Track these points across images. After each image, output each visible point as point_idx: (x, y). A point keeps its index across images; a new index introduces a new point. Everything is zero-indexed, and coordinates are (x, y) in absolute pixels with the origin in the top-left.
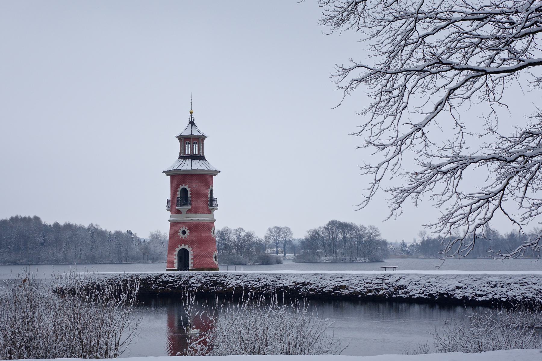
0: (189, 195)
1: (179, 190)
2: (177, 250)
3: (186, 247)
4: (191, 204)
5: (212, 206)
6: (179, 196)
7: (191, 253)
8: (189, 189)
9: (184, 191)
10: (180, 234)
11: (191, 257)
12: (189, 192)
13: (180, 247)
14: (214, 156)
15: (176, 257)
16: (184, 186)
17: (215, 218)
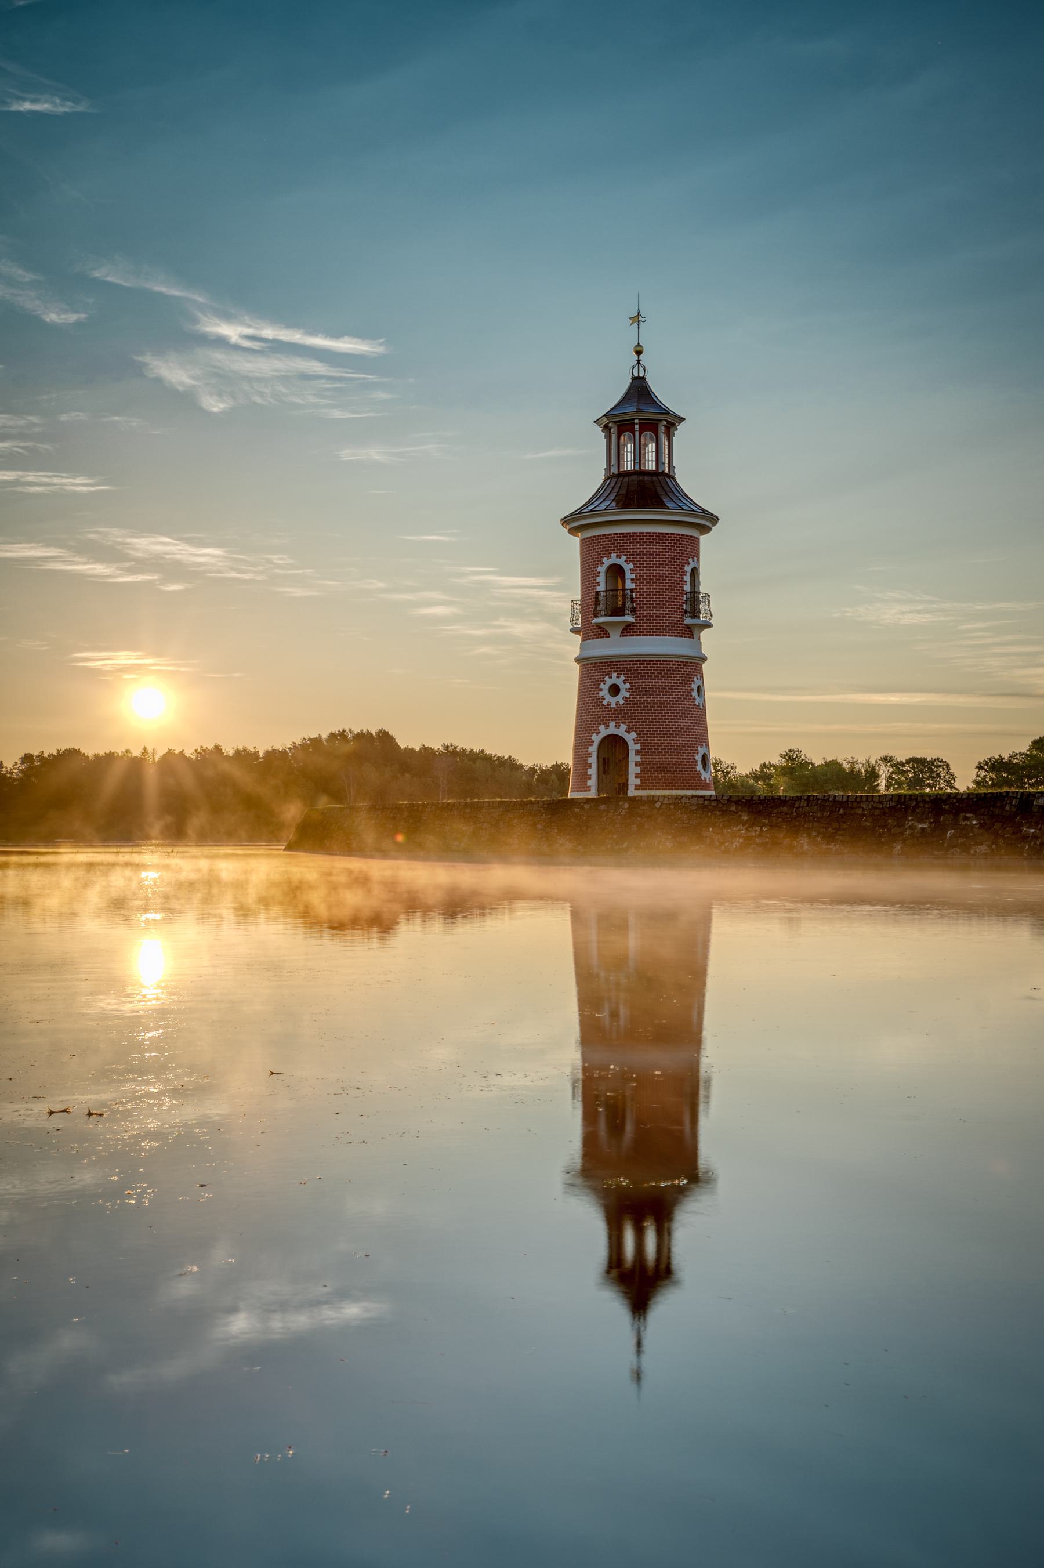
0: (630, 585)
1: (601, 569)
3: (621, 731)
4: (634, 611)
5: (695, 613)
6: (601, 588)
7: (633, 747)
8: (628, 567)
9: (616, 571)
10: (605, 693)
11: (633, 758)
12: (629, 576)
13: (604, 731)
14: (696, 467)
16: (614, 559)
17: (704, 651)
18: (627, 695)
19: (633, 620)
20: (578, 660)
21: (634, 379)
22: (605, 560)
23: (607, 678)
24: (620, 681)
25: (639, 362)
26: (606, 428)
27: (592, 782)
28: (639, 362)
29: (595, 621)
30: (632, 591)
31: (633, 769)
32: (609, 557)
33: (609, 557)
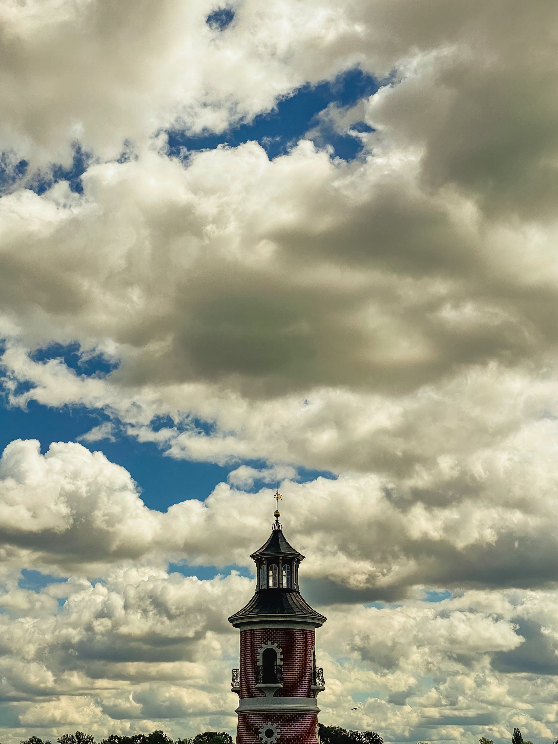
0: (279, 663)
1: (261, 651)
4: (282, 679)
6: (260, 663)
8: (279, 651)
12: (279, 656)
16: (269, 645)
18: (279, 737)
19: (282, 686)
20: (237, 712)
21: (273, 531)
22: (263, 645)
23: (264, 725)
24: (273, 727)
25: (277, 521)
28: (277, 521)
29: (257, 686)
30: (281, 666)
32: (266, 644)
33: (266, 644)
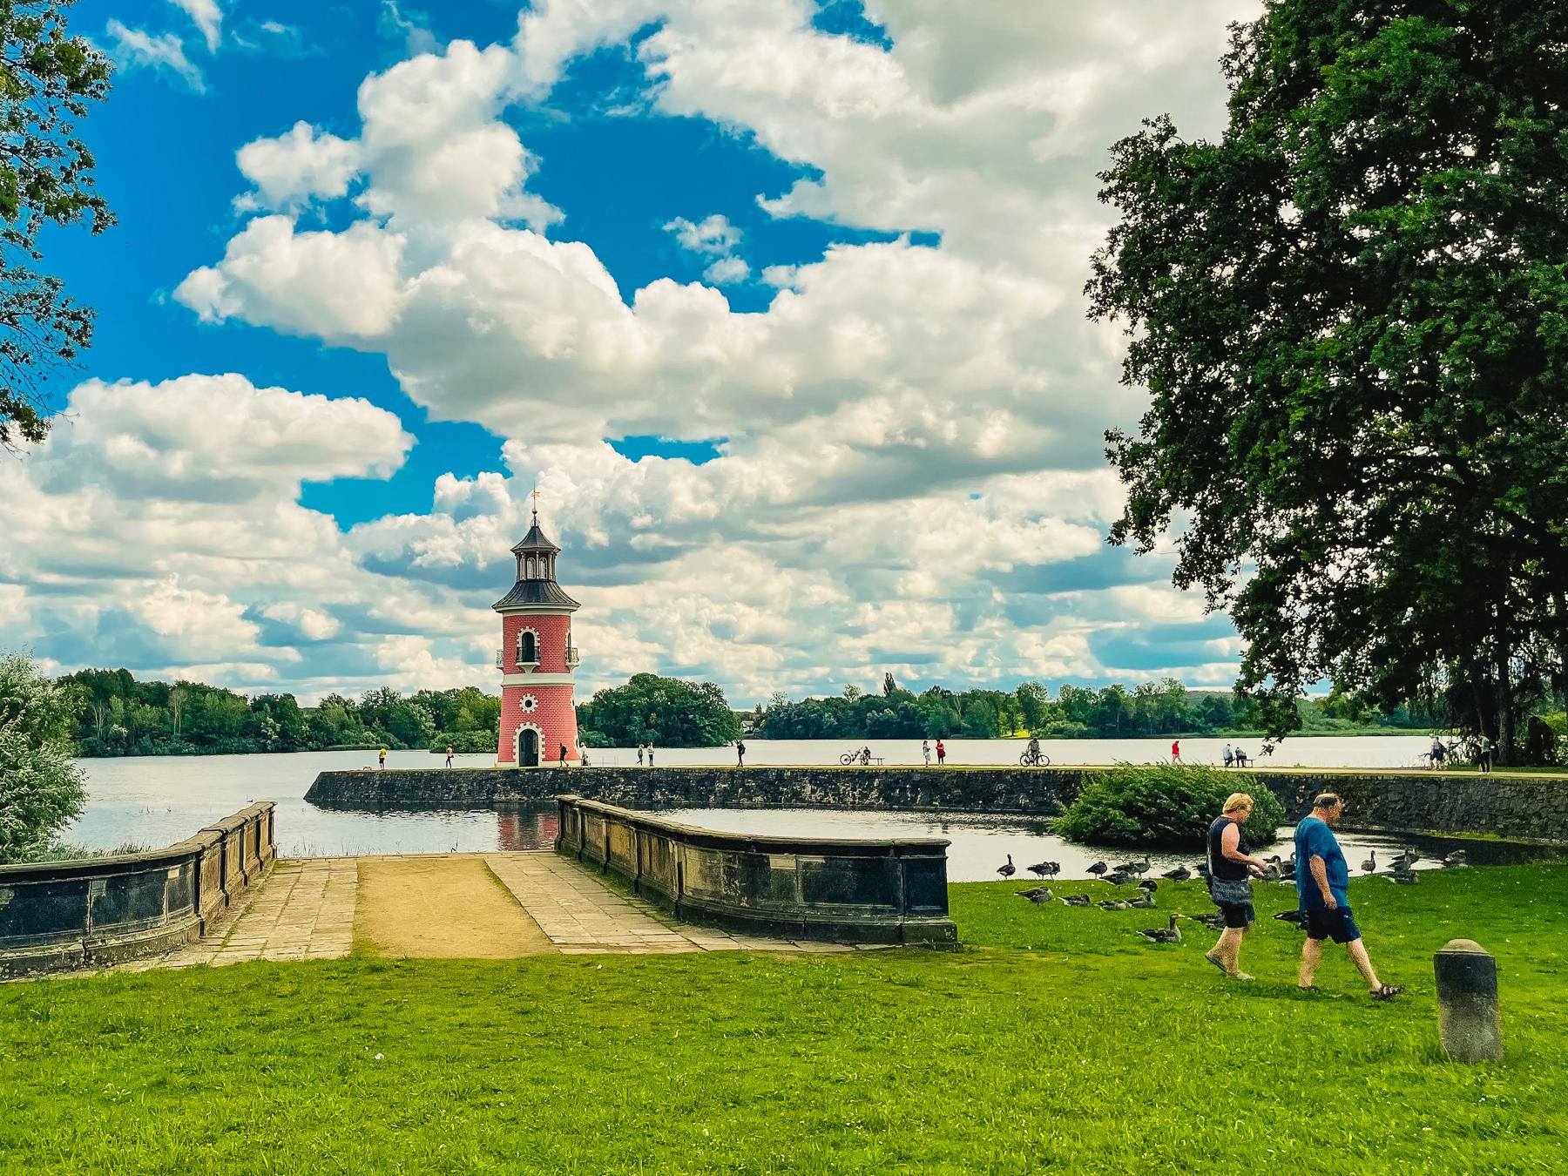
2: (519, 732)
3: (533, 727)
7: (541, 737)
8: (535, 634)
9: (528, 638)
11: (541, 743)
13: (523, 728)
15: (517, 744)
16: (528, 630)
26: (519, 556)
27: (517, 757)
31: (541, 749)
